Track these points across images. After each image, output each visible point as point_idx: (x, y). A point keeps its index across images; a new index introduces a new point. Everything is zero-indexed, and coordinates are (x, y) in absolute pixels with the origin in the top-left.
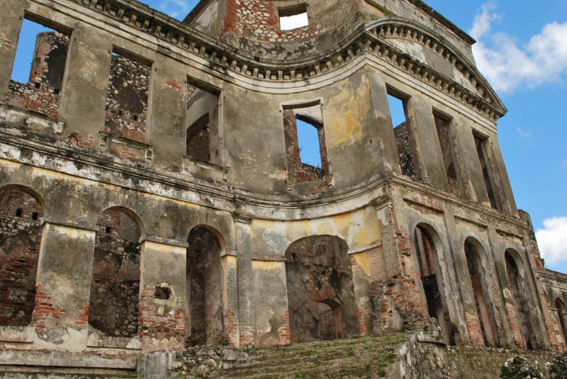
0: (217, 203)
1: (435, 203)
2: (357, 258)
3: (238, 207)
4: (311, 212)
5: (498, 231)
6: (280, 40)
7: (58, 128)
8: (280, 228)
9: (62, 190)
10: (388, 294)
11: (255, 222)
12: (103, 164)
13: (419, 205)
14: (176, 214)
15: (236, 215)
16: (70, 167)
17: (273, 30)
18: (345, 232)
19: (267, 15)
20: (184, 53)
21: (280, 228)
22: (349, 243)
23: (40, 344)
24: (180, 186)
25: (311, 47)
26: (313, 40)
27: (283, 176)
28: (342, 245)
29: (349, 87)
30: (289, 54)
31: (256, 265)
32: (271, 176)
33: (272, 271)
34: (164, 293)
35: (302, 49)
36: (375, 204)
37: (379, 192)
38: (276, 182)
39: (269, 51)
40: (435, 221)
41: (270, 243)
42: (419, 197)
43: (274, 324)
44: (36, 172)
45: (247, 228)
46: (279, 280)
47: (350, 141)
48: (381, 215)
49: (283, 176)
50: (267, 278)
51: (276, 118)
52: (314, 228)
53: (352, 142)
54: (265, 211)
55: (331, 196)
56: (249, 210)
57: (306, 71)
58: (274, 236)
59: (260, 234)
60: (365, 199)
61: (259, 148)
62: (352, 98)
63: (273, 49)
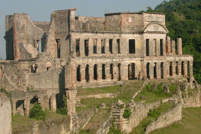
0: (120, 59)
2: (138, 67)
3: (123, 59)
4: (132, 59)
6: (129, 25)
7: (106, 55)
8: (127, 61)
9: (107, 62)
10: (142, 73)
11: (125, 61)
12: (110, 58)
14: (116, 62)
15: (122, 61)
16: (107, 60)
18: (137, 63)
19: (127, 18)
20: (116, 35)
21: (127, 61)
23: (107, 81)
24: (117, 58)
25: (134, 28)
26: (135, 26)
31: (124, 67)
37: (142, 59)
39: (127, 28)
40: (150, 62)
41: (126, 64)
42: (148, 59)
44: (105, 61)
45: (123, 62)
47: (139, 48)
48: (142, 62)
51: (127, 42)
52: (133, 62)
53: (140, 48)
54: (126, 59)
56: (124, 59)
57: (133, 33)
58: (127, 63)
59: (125, 62)
60: (140, 59)
61: (125, 48)
63: (128, 27)
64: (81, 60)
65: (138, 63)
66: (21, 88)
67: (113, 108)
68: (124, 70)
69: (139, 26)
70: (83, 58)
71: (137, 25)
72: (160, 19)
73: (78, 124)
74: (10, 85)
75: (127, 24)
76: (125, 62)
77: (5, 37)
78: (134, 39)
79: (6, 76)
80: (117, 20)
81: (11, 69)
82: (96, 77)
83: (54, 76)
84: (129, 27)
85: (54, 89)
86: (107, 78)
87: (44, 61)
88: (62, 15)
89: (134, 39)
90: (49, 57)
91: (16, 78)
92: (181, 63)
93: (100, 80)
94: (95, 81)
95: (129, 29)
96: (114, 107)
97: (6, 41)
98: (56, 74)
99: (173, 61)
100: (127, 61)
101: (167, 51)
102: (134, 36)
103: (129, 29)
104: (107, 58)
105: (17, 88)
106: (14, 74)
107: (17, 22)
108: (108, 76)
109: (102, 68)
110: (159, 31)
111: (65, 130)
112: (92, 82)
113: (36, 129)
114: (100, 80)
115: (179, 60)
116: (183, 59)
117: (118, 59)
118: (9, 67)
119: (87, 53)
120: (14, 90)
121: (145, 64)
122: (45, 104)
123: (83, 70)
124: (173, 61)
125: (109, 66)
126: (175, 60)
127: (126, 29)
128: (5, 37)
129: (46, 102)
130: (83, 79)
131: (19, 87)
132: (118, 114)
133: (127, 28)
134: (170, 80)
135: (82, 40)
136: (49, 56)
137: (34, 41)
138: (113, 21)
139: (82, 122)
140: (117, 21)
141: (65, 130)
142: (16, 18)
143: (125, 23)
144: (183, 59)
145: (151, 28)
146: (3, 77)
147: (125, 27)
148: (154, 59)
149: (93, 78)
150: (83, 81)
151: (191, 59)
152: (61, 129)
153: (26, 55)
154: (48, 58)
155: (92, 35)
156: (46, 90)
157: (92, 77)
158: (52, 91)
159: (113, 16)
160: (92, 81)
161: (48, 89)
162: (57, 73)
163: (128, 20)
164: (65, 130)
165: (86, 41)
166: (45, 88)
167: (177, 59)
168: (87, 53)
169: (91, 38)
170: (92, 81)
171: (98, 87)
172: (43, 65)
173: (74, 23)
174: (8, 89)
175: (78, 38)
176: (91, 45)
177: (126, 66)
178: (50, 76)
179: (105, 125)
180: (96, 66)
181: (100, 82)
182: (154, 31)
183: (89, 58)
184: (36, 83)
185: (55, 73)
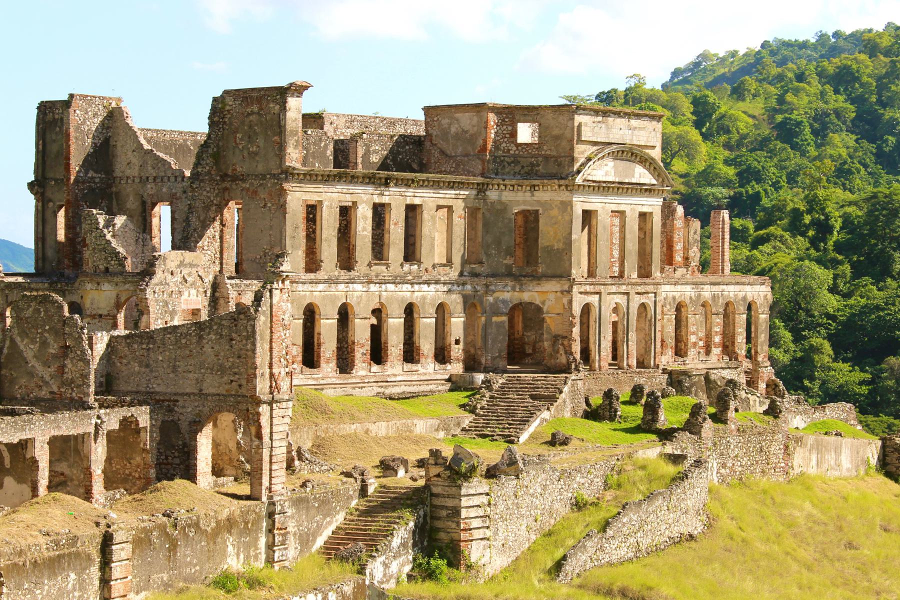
0: (478, 288)
1: (597, 288)
5: (638, 293)
6: (517, 152)
12: (437, 282)
13: (586, 293)
16: (425, 287)
17: (512, 142)
18: (543, 303)
19: (510, 128)
22: (545, 310)
23: (422, 371)
27: (509, 261)
28: (539, 309)
29: (559, 208)
30: (523, 167)
31: (495, 319)
32: (505, 262)
33: (501, 322)
34: (457, 342)
35: (532, 165)
36: (562, 292)
37: (566, 287)
38: (507, 266)
39: (509, 164)
41: (501, 305)
43: (500, 352)
45: (491, 299)
46: (504, 327)
49: (509, 261)
50: (499, 325)
52: (526, 297)
54: (500, 286)
55: (538, 278)
58: (504, 302)
59: (496, 300)
62: (560, 217)
63: (512, 162)
64: (321, 287)
65: (548, 303)
66: (72, 389)
67: (436, 479)
68: (493, 330)
69: (556, 161)
70: (330, 281)
71: (548, 152)
72: (642, 133)
73: (295, 534)
74: (31, 374)
75: (509, 150)
76: (496, 300)
77: (31, 186)
78: (538, 211)
79: (18, 340)
80: (471, 132)
81: (39, 311)
82: (378, 355)
83: (207, 346)
84: (516, 162)
85: (207, 395)
86: (423, 360)
87: (171, 284)
88: (255, 108)
89: (538, 211)
90: (194, 270)
91: (53, 349)
92: (721, 310)
93: (395, 368)
94: (375, 368)
95: (517, 169)
96: (438, 476)
97: (37, 201)
98: (214, 337)
99: (691, 298)
100: (506, 296)
101: (668, 259)
102: (535, 198)
103: (517, 169)
104: (428, 283)
105: (59, 388)
106: (46, 335)
107: (78, 128)
108: (426, 352)
109: (403, 320)
110: (634, 181)
111: (242, 556)
112: (363, 373)
113: (122, 549)
114: (395, 368)
115: (714, 297)
116: (732, 295)
117: (469, 287)
118: (29, 306)
119: (346, 261)
120: (48, 396)
121: (577, 310)
122: (168, 453)
123: (327, 324)
124: (691, 298)
125: (433, 311)
126: (700, 295)
127: (507, 170)
128: (31, 186)
129: (173, 446)
130: (328, 361)
131: (63, 384)
132: (450, 503)
133: (509, 164)
134: (670, 373)
135: (331, 207)
136: (191, 265)
137: (144, 203)
138: (457, 137)
139: (309, 530)
140: (472, 135)
141: (238, 555)
142: (78, 112)
143: (504, 145)
144: (732, 295)
145: (604, 170)
146: (8, 343)
147: (502, 161)
148: (614, 289)
149: (369, 357)
150: (328, 368)
151: (762, 294)
152: (224, 555)
153: (106, 258)
154: (190, 274)
155: (370, 189)
156: (176, 398)
157: (363, 354)
158: (196, 404)
159: (457, 115)
160: (362, 368)
161: (183, 394)
162: (216, 334)
163: (514, 134)
164: (242, 556)
165: (346, 213)
166: (169, 390)
167: (707, 292)
168: (346, 261)
169: (365, 202)
170: (363, 369)
171: (387, 392)
172: (166, 304)
173: (297, 141)
174: (24, 390)
175: (313, 198)
176: (364, 229)
177: (502, 314)
178: (191, 344)
179: (399, 541)
180: (344, 315)
181: (395, 375)
182: (617, 180)
183: (352, 281)
184: (137, 369)
185: (209, 334)
